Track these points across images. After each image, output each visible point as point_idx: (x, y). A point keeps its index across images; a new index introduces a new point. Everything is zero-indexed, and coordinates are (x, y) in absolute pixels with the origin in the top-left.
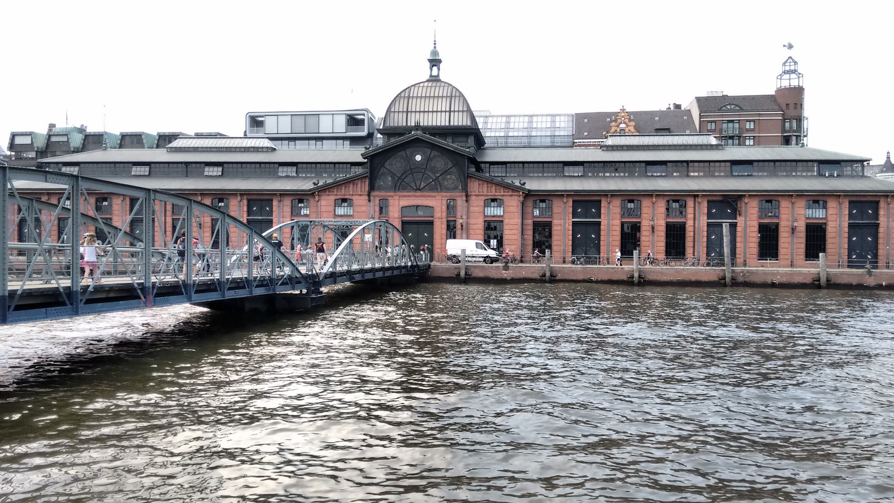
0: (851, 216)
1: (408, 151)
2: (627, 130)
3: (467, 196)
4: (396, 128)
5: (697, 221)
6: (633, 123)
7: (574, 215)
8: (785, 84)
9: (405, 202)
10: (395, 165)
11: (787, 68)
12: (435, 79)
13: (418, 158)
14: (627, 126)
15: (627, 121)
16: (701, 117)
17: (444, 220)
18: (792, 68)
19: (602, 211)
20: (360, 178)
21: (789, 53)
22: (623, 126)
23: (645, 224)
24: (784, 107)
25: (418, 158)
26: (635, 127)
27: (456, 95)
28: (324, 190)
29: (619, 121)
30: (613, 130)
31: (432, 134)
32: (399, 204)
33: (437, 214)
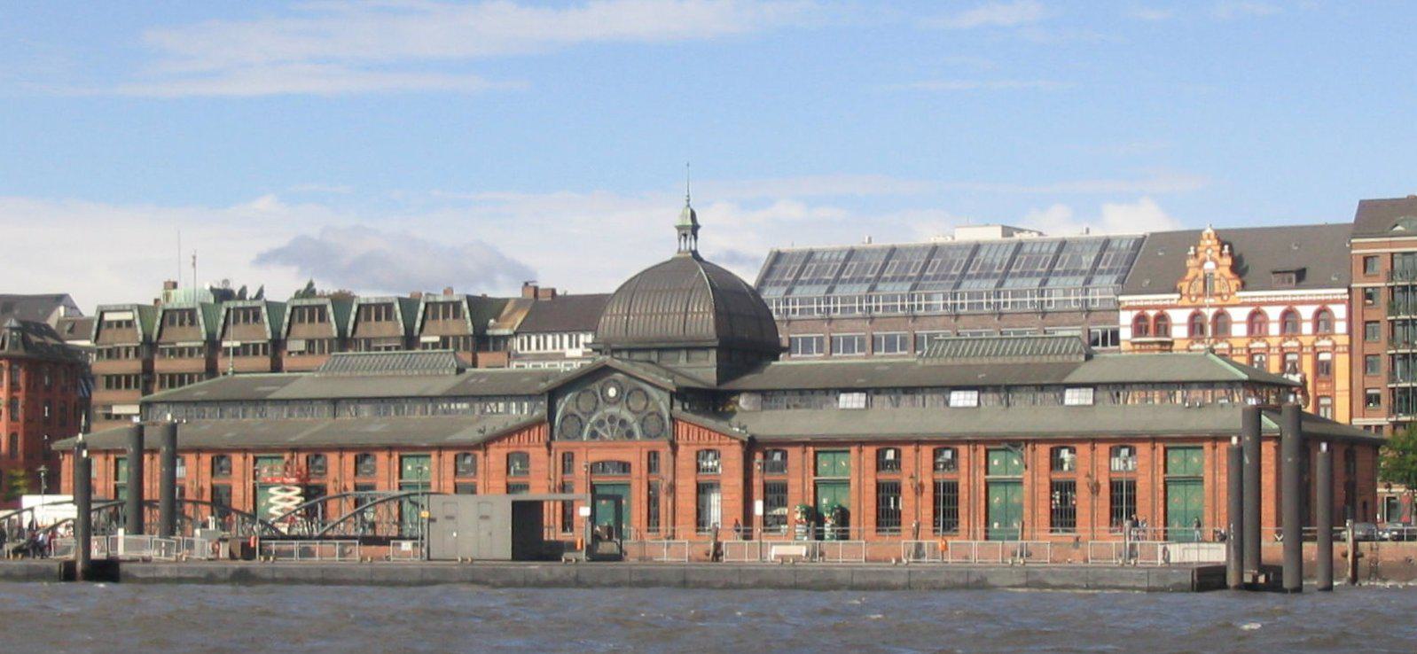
2: (1217, 276)
6: (1227, 261)
9: (597, 456)
14: (1218, 266)
15: (1216, 255)
22: (1209, 266)
29: (1201, 256)
30: (1190, 275)
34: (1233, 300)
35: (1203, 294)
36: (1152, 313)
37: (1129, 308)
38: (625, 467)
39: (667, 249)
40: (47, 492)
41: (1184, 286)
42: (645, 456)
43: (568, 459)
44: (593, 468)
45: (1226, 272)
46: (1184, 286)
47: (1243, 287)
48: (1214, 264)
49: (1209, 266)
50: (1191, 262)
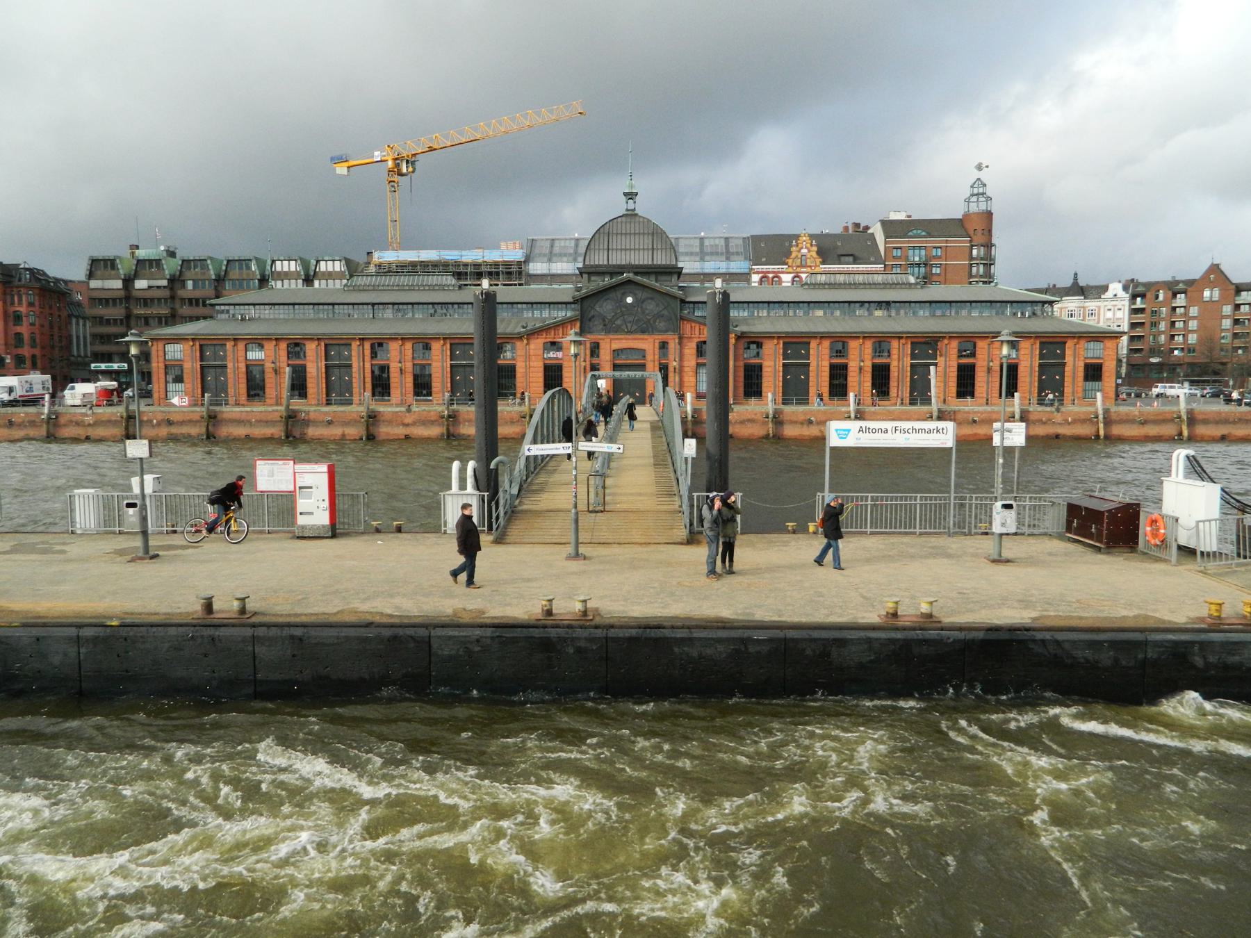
0: (1042, 356)
1: (619, 294)
3: (681, 338)
4: (597, 266)
5: (900, 361)
6: (815, 249)
7: (785, 356)
8: (974, 208)
9: (615, 346)
10: (605, 307)
11: (976, 191)
12: (631, 215)
13: (629, 300)
16: (886, 242)
17: (657, 364)
18: (981, 190)
19: (812, 352)
20: (571, 321)
21: (977, 174)
22: (804, 251)
23: (853, 365)
24: (971, 233)
25: (629, 300)
26: (818, 253)
27: (657, 233)
28: (533, 334)
30: (793, 255)
31: (636, 273)
32: (610, 344)
33: (649, 357)
34: (818, 270)
35: (801, 266)
36: (771, 276)
37: (758, 273)
38: (642, 352)
39: (620, 206)
40: (831, 385)
41: (790, 261)
42: (657, 345)
43: (595, 349)
44: (617, 352)
45: (814, 254)
46: (790, 261)
47: (823, 263)
48: (806, 250)
49: (804, 251)
50: (794, 249)
